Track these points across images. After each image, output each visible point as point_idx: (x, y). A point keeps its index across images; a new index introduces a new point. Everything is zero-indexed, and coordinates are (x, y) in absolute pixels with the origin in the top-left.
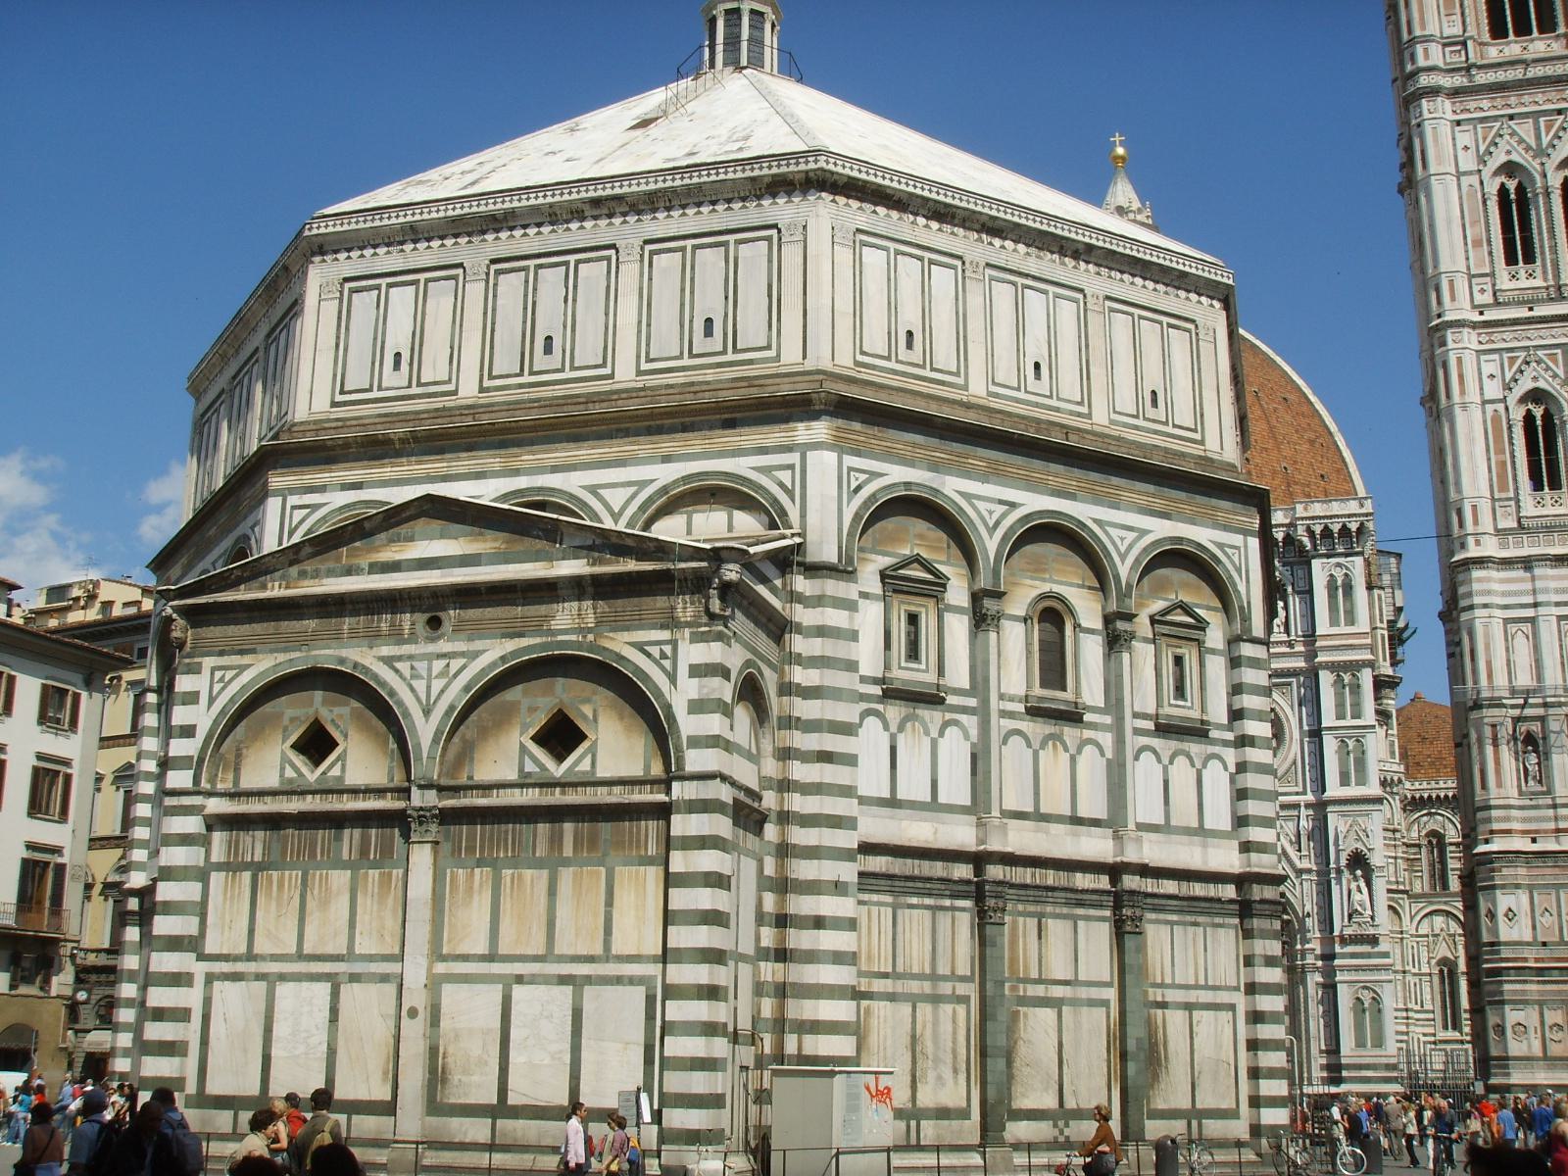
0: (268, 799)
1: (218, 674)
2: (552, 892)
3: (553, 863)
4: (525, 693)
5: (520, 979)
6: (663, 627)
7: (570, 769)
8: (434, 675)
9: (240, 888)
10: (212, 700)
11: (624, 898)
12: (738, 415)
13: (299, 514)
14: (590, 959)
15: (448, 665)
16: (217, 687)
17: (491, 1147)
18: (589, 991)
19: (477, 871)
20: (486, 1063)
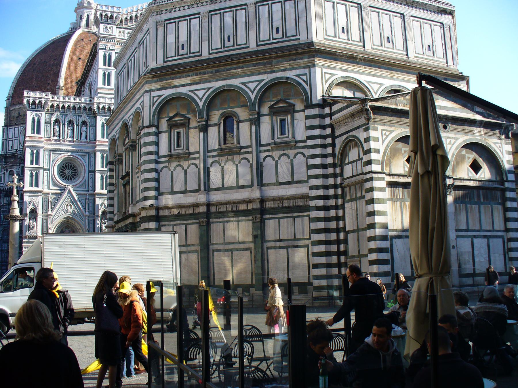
0: (401, 177)
1: (384, 132)
2: (480, 212)
3: (479, 203)
4: (467, 153)
5: (475, 237)
6: (499, 139)
7: (480, 176)
8: (447, 143)
9: (397, 207)
10: (383, 141)
11: (496, 214)
12: (447, 77)
13: (328, 76)
14: (489, 231)
15: (451, 141)
16: (384, 137)
17: (473, 285)
18: (491, 240)
19: (461, 204)
20: (469, 261)
